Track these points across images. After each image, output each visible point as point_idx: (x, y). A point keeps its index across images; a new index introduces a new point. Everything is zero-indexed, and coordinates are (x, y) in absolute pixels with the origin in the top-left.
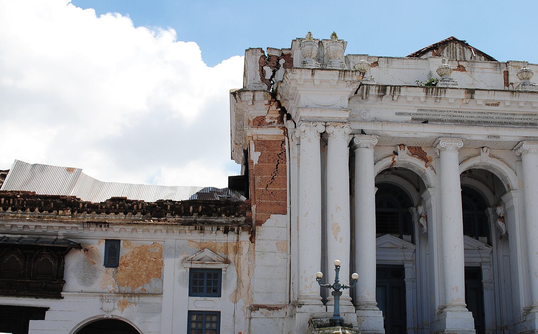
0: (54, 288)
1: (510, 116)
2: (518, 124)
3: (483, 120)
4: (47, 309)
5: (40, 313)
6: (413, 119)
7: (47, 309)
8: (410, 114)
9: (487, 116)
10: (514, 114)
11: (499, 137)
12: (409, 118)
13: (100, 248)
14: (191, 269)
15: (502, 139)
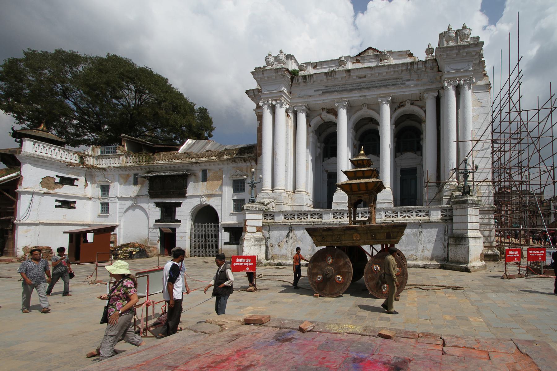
0: (183, 194)
2: (376, 87)
4: (181, 203)
5: (179, 205)
7: (181, 203)
11: (365, 96)
13: (200, 174)
14: (234, 181)
15: (367, 97)
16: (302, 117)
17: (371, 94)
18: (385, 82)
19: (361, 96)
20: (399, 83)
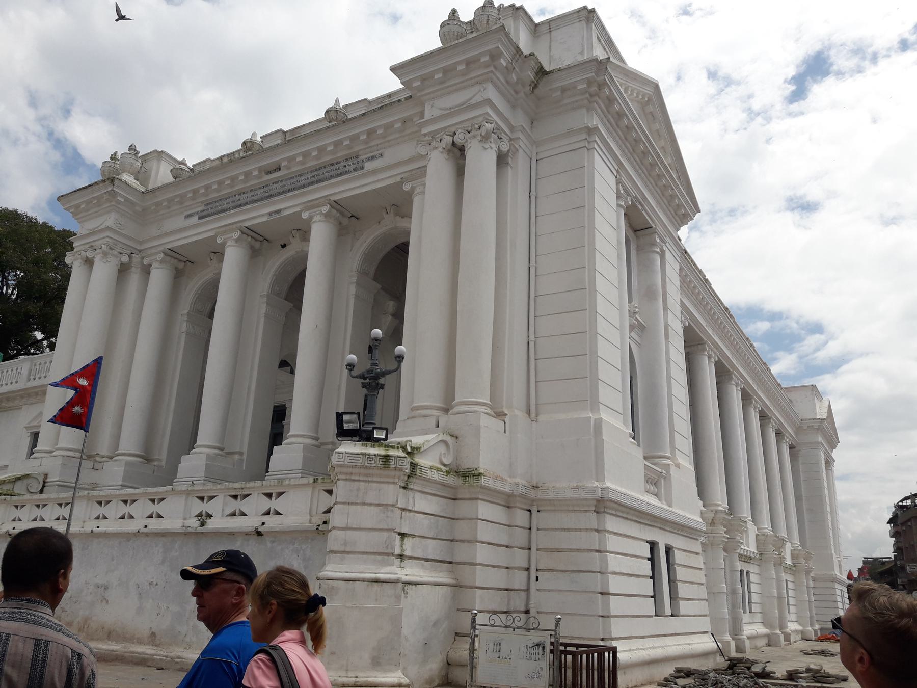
1: (296, 179)
3: (267, 194)
6: (200, 218)
8: (197, 213)
9: (270, 188)
10: (300, 175)
11: (280, 211)
12: (196, 217)
15: (286, 213)
16: (159, 277)
17: (289, 205)
18: (321, 172)
19: (270, 214)
20: (351, 168)
